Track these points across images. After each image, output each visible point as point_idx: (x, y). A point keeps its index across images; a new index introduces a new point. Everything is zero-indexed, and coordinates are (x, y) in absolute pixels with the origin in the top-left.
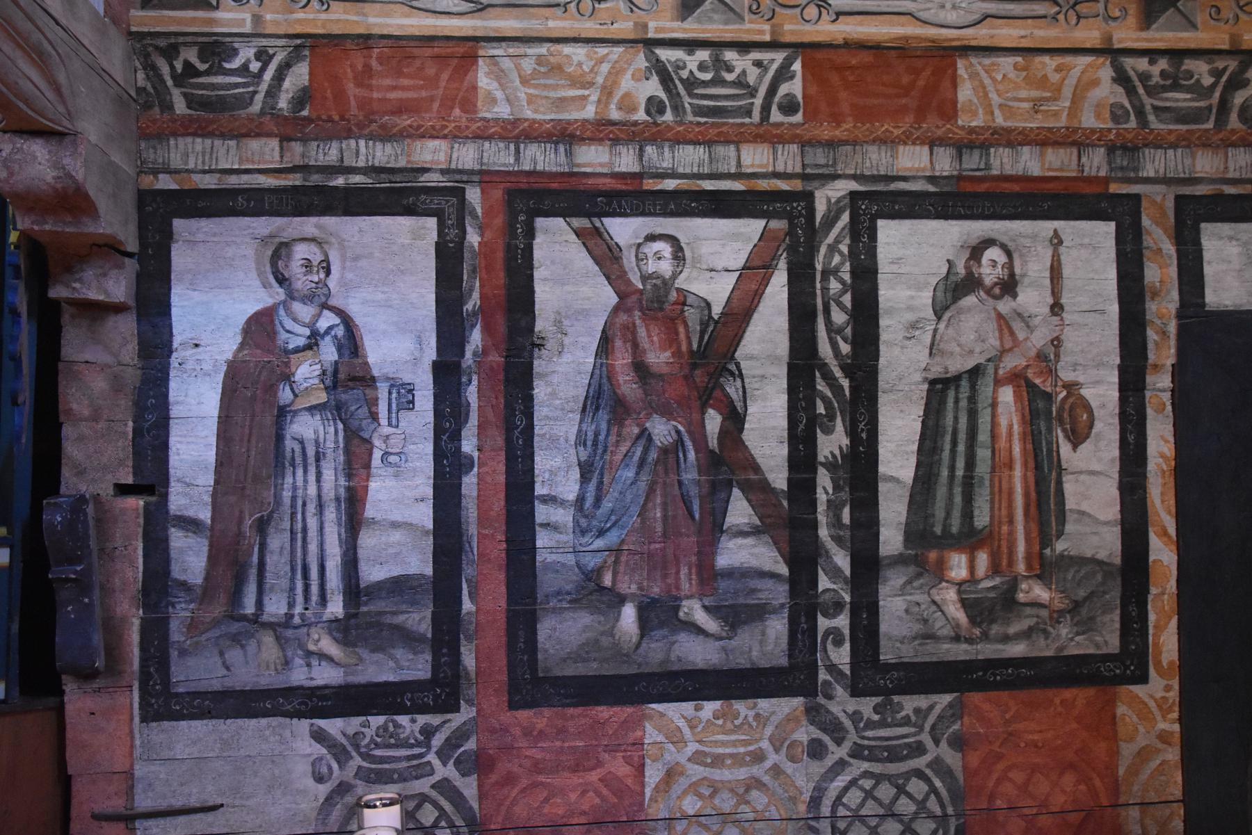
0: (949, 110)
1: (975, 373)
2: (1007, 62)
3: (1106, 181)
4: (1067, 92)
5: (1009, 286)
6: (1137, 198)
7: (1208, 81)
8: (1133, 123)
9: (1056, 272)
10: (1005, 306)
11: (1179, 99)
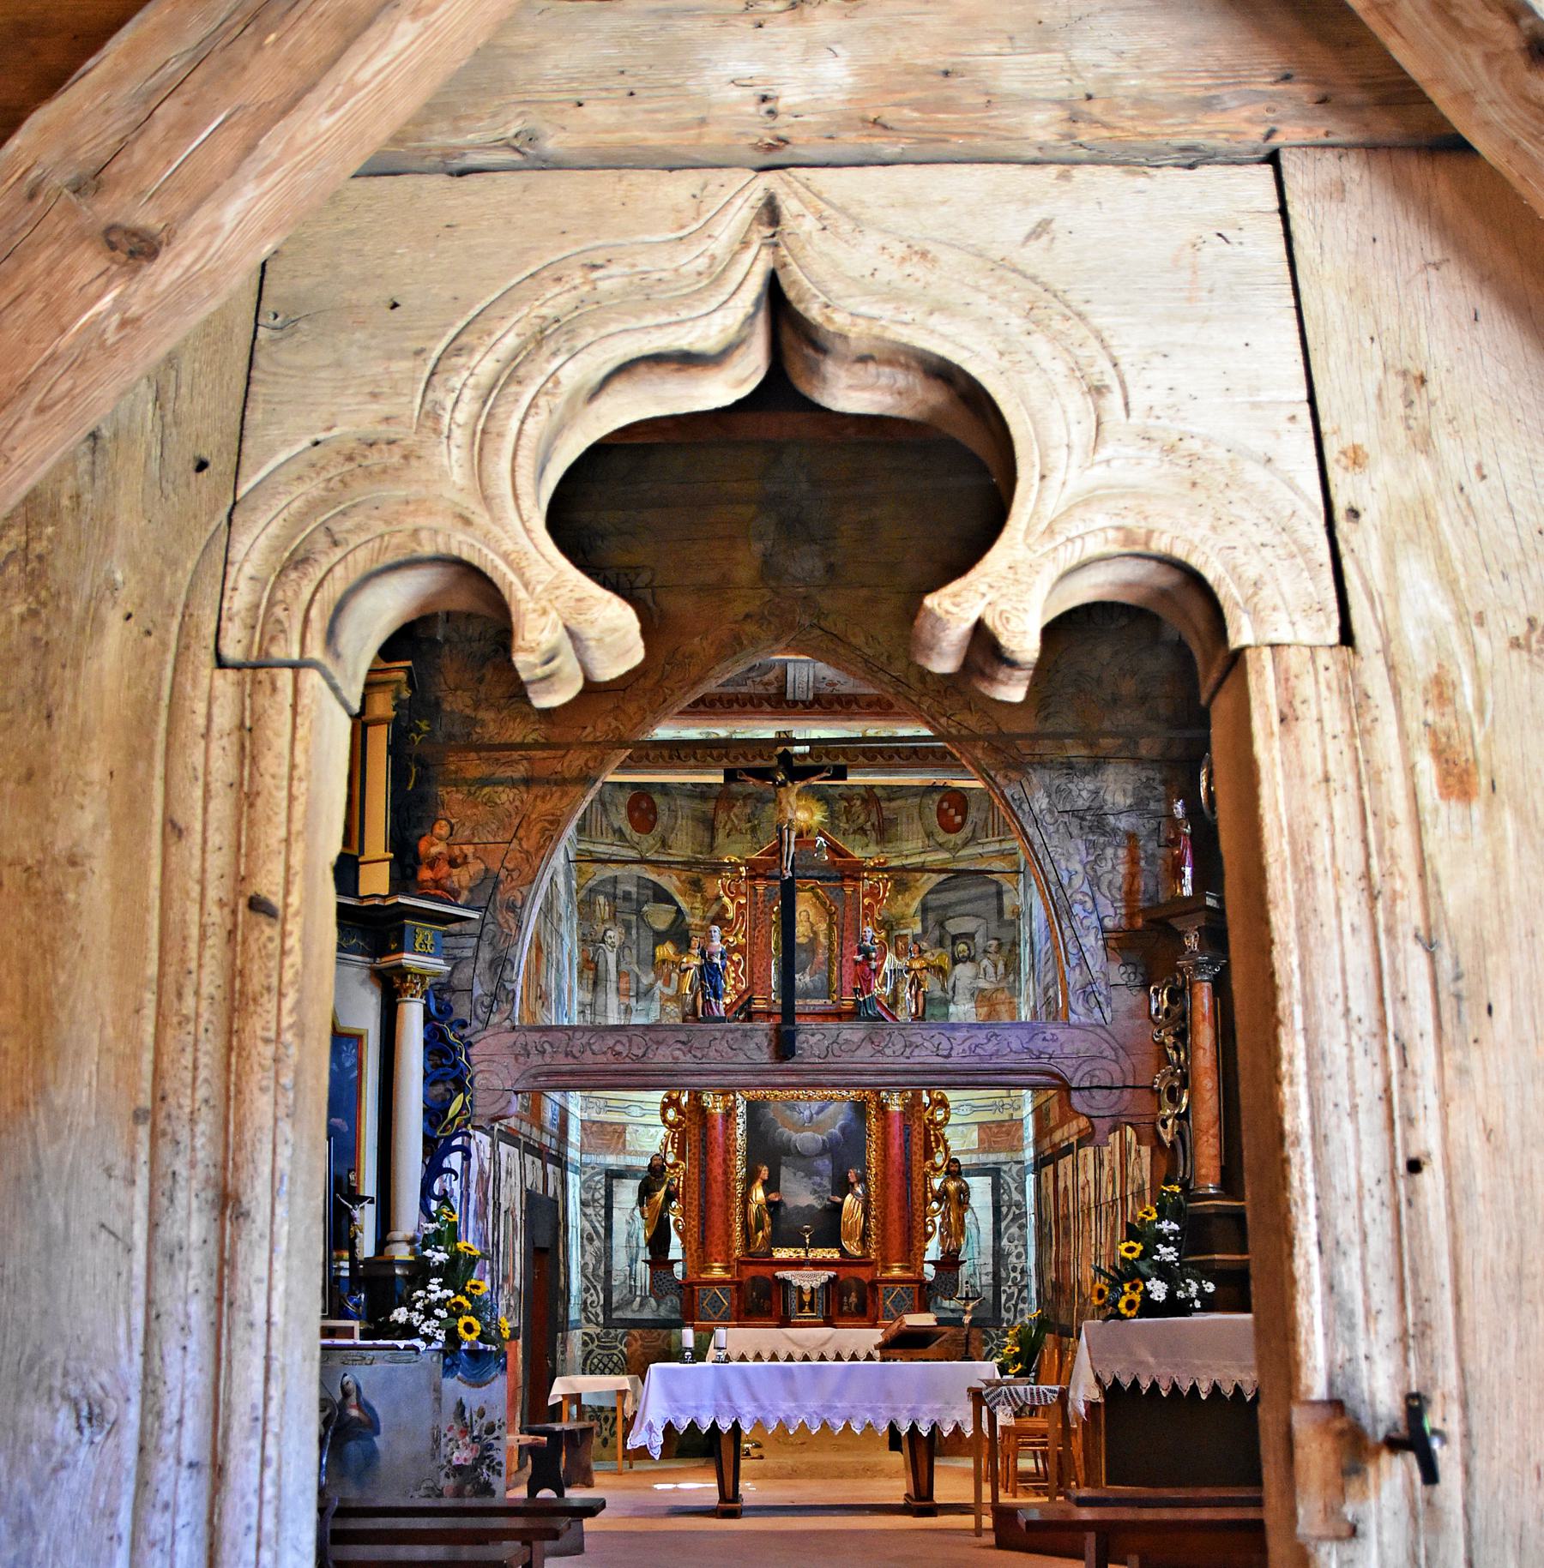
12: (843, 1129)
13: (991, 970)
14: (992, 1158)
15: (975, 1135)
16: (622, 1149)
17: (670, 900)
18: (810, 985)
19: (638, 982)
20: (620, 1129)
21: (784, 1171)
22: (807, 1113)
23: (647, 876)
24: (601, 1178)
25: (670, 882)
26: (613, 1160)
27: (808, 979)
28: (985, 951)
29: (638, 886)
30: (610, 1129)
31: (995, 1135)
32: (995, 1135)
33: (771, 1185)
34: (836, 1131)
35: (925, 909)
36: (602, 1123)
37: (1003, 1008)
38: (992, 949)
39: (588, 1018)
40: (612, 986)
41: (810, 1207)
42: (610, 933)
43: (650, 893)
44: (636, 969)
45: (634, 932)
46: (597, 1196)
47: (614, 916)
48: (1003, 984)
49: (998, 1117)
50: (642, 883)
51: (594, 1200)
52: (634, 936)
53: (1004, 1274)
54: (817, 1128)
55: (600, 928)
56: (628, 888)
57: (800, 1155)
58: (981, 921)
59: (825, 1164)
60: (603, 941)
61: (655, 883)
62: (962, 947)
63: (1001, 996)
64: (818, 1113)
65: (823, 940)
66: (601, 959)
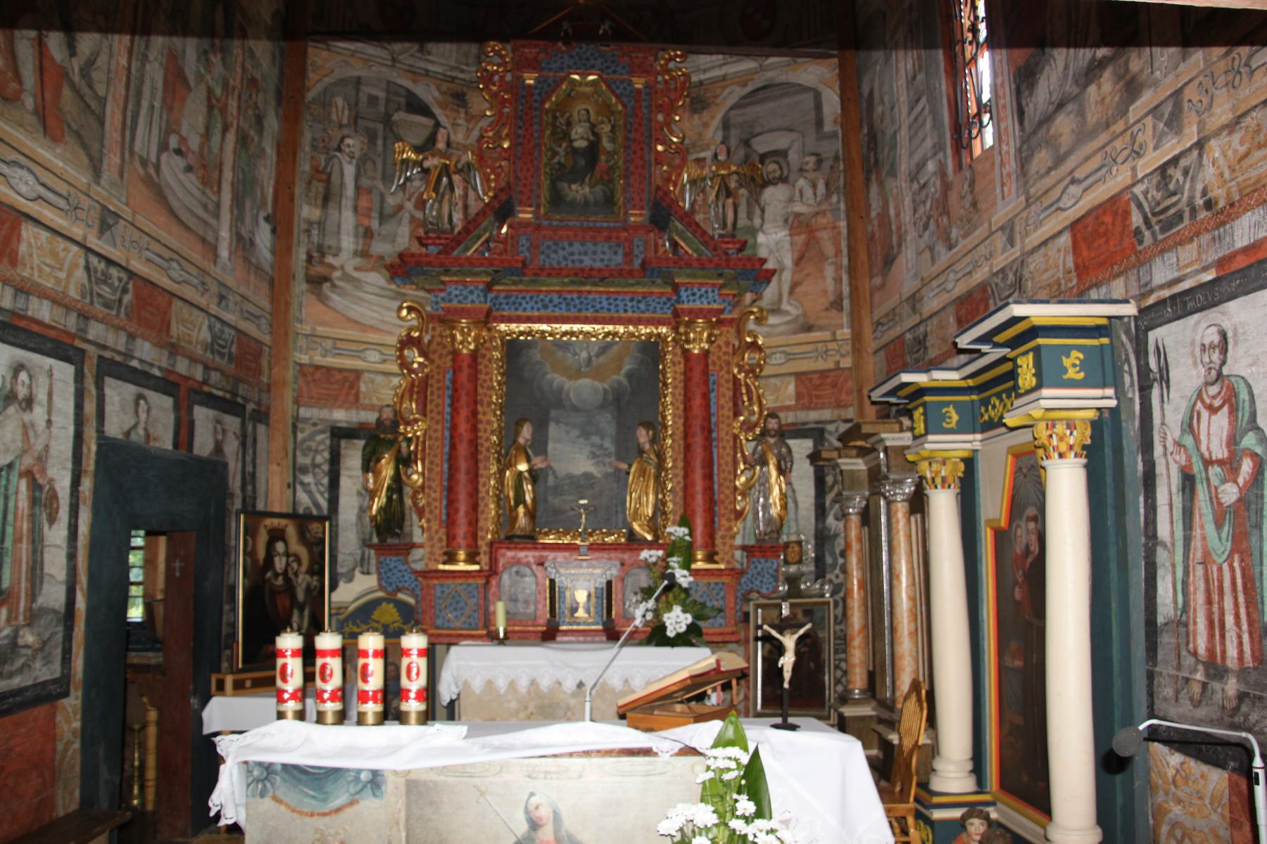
0: (14, 261)
1: (10, 466)
2: (45, 235)
3: (74, 336)
4: (66, 267)
5: (29, 403)
6: (83, 351)
7: (116, 284)
8: (87, 301)
9: (50, 395)
10: (27, 417)
11: (105, 291)
12: (630, 376)
13: (808, 192)
14: (813, 415)
15: (791, 388)
16: (354, 400)
17: (425, 111)
18: (591, 198)
19: (382, 201)
20: (352, 377)
21: (553, 430)
22: (584, 355)
23: (400, 81)
24: (324, 439)
25: (428, 93)
26: (341, 416)
27: (587, 189)
28: (801, 170)
29: (388, 92)
30: (338, 376)
31: (817, 387)
32: (817, 387)
33: (540, 445)
34: (621, 377)
35: (726, 125)
36: (329, 370)
37: (824, 235)
38: (811, 166)
39: (315, 239)
40: (347, 203)
41: (587, 476)
42: (349, 141)
43: (402, 100)
44: (381, 186)
45: (380, 142)
46: (319, 459)
47: (355, 119)
48: (824, 207)
49: (821, 365)
50: (391, 88)
51: (315, 466)
52: (380, 148)
53: (829, 560)
54: (597, 374)
55: (336, 134)
56: (374, 92)
57: (575, 409)
58: (794, 135)
59: (606, 421)
60: (339, 149)
61: (408, 91)
62: (772, 167)
63: (822, 221)
64: (598, 356)
65: (606, 144)
66: (336, 169)
